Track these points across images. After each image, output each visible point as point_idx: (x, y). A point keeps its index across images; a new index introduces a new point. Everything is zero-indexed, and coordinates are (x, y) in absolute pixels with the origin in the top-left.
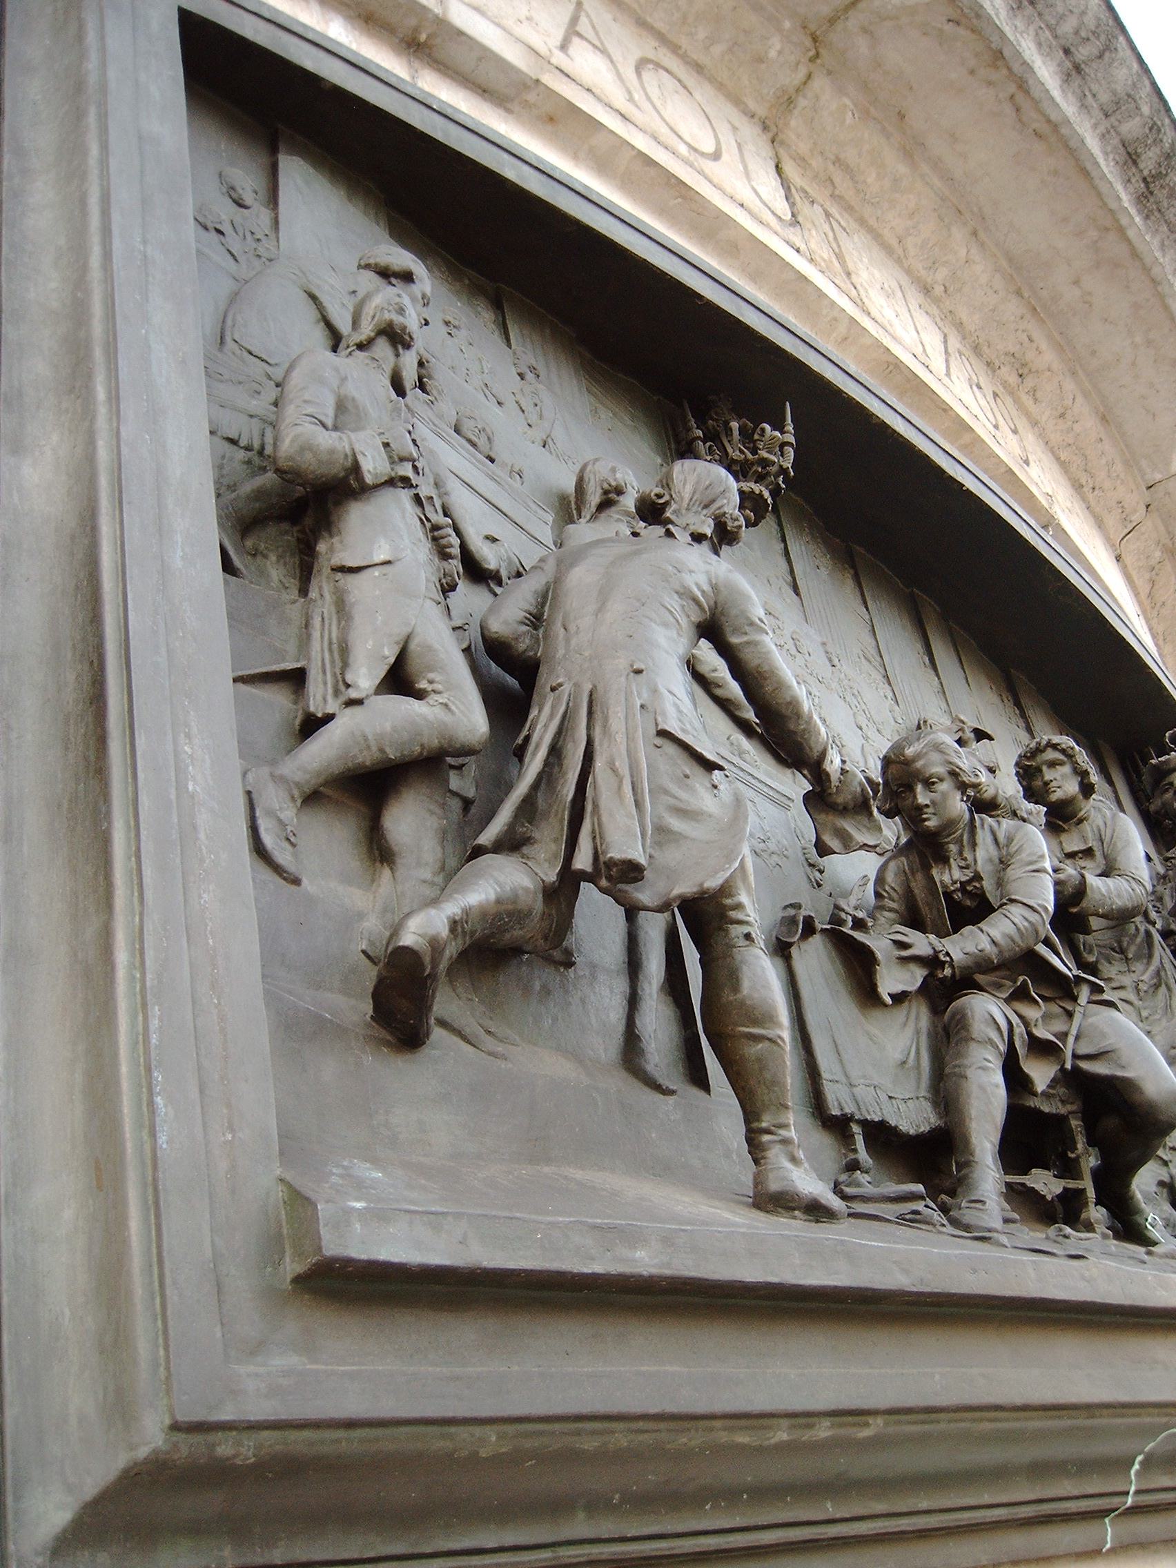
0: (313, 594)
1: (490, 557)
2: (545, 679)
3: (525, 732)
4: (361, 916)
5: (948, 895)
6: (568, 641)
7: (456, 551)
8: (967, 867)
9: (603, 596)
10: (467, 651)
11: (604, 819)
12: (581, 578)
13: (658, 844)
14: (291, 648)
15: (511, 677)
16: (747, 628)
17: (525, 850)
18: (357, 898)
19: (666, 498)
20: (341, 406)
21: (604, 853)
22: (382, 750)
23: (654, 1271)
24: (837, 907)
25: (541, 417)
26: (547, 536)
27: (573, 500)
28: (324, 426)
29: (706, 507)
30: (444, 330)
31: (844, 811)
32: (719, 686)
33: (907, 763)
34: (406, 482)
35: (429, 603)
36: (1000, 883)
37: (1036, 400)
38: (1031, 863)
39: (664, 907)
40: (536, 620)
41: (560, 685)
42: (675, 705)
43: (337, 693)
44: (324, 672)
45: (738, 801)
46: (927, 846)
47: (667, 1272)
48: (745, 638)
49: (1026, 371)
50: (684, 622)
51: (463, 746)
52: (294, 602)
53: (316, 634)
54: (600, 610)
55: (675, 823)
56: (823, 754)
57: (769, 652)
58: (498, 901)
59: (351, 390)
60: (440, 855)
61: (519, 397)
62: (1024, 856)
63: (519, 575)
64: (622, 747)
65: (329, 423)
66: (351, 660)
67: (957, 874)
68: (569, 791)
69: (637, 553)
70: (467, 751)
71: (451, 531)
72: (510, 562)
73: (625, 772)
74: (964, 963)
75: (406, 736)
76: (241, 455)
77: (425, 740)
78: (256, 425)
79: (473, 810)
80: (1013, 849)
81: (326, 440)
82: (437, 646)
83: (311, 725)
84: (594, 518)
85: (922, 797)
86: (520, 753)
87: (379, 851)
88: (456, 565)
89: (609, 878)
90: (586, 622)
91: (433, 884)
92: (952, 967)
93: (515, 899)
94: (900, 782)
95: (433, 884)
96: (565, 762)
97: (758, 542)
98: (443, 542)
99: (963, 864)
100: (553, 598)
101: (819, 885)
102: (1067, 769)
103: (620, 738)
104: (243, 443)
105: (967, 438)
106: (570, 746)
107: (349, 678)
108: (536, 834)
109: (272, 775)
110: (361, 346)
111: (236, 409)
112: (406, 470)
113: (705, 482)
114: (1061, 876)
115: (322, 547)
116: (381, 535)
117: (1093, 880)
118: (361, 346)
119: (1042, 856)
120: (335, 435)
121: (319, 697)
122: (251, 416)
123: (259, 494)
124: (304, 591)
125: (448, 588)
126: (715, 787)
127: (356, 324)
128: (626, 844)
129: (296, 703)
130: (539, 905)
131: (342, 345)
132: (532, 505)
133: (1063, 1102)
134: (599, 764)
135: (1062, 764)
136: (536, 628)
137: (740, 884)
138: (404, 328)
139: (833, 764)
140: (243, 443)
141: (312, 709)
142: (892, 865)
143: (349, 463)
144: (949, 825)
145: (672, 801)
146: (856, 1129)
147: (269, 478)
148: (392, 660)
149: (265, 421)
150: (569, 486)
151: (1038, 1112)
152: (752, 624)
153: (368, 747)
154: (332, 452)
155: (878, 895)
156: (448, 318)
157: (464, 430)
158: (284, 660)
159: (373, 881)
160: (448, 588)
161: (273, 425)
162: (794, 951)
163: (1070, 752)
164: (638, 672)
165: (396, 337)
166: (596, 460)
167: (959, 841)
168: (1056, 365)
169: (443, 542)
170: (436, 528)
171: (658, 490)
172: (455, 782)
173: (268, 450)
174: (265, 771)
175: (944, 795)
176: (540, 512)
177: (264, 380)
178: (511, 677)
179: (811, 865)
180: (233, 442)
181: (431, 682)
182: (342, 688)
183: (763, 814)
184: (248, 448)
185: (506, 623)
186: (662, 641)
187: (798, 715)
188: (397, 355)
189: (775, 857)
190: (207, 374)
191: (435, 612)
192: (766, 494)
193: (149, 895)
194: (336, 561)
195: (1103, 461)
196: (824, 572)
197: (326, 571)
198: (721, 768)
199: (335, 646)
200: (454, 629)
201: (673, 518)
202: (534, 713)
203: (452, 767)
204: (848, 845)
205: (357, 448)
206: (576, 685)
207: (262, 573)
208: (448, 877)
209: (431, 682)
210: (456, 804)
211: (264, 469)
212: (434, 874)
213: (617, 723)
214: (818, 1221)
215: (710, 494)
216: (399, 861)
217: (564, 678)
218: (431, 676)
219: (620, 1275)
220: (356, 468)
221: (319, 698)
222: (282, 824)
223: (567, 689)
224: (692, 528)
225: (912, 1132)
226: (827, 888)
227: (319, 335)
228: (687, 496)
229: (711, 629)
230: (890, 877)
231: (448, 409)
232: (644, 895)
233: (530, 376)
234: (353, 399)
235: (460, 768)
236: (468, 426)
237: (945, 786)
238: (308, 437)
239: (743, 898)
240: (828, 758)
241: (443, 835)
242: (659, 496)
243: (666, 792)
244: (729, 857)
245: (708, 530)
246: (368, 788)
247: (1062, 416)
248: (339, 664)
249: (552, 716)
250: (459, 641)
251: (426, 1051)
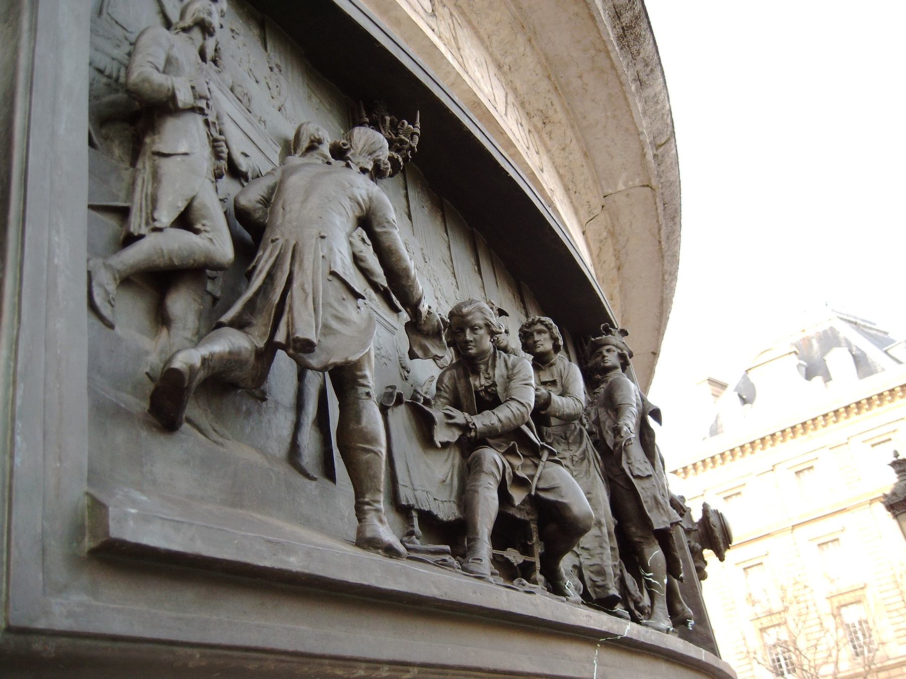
0: (139, 165)
1: (244, 165)
2: (268, 235)
3: (254, 264)
4: (147, 353)
5: (477, 392)
6: (284, 216)
7: (225, 156)
8: (489, 378)
9: (308, 193)
10: (225, 213)
11: (296, 315)
12: (295, 182)
13: (324, 335)
14: (123, 195)
15: (250, 229)
16: (386, 224)
17: (247, 329)
18: (146, 342)
19: (348, 146)
20: (169, 61)
21: (293, 334)
22: (171, 259)
23: (299, 570)
24: (416, 391)
25: (279, 94)
26: (276, 160)
27: (292, 143)
28: (158, 69)
29: (370, 154)
30: (230, 34)
31: (427, 335)
32: (362, 261)
33: (464, 316)
34: (201, 111)
35: (207, 181)
36: (506, 389)
37: (551, 138)
38: (524, 380)
39: (323, 370)
40: (267, 202)
41: (277, 239)
42: (341, 259)
43: (147, 224)
44: (141, 211)
45: (370, 318)
46: (468, 363)
47: (306, 571)
48: (384, 230)
49: (547, 121)
50: (351, 214)
51: (218, 263)
52: (126, 169)
53: (138, 189)
54: (305, 200)
55: (334, 324)
56: (420, 300)
57: (395, 239)
58: (230, 353)
59: (175, 52)
60: (197, 325)
61: (268, 80)
62: (521, 375)
63: (258, 177)
64: (309, 277)
65: (161, 68)
66: (158, 206)
67: (483, 382)
68: (276, 298)
69: (328, 173)
70: (219, 267)
71: (223, 144)
72: (254, 170)
73: (310, 291)
75: (186, 253)
76: (104, 80)
77: (197, 258)
78: (115, 65)
79: (218, 304)
80: (515, 371)
81: (158, 78)
82: (210, 205)
83: (130, 239)
84: (303, 155)
85: (469, 336)
86: (249, 276)
87: (161, 318)
88: (224, 164)
89: (295, 349)
90: (296, 206)
91: (191, 341)
92: (476, 431)
93: (239, 353)
94: (458, 326)
95: (191, 341)
96: (276, 282)
97: (393, 184)
98: (219, 149)
99: (487, 376)
100: (279, 191)
101: (406, 379)
102: (547, 336)
103: (309, 272)
104: (107, 73)
105: (512, 151)
106: (279, 273)
107: (156, 216)
108: (254, 322)
109: (104, 264)
110: (185, 30)
111: (104, 53)
112: (202, 104)
113: (371, 141)
114: (538, 393)
115: (148, 140)
116: (183, 138)
117: (555, 397)
118: (185, 30)
119: (531, 377)
120: (164, 76)
121: (137, 224)
122: (113, 59)
123: (112, 104)
124: (133, 164)
125: (218, 176)
126: (359, 308)
127: (182, 16)
128: (306, 330)
129: (122, 226)
130: (252, 359)
131: (172, 28)
132: (271, 142)
133: (528, 513)
134: (295, 285)
135: (545, 332)
136: (266, 207)
137: (366, 365)
138: (210, 24)
139: (424, 308)
140: (107, 73)
141: (132, 230)
142: (448, 373)
143: (170, 94)
144: (482, 353)
145: (334, 312)
146: (414, 514)
147: (121, 96)
148: (182, 209)
149: (121, 63)
150: (291, 136)
152: (388, 222)
153: (163, 256)
154: (161, 85)
155: (438, 389)
156: (234, 28)
157: (236, 91)
158: (117, 200)
159: (156, 335)
160: (218, 176)
161: (127, 67)
162: (390, 412)
164: (323, 237)
165: (205, 28)
166: (309, 123)
167: (486, 364)
168: (564, 121)
169: (219, 149)
170: (215, 140)
171: (344, 141)
172: (210, 287)
173: (122, 80)
174: (100, 261)
175: (481, 337)
176: (274, 146)
177: (123, 39)
178: (250, 229)
179: (403, 368)
180: (101, 71)
181: (204, 225)
182: (151, 221)
183: (380, 334)
184: (109, 77)
185: (249, 201)
186: (338, 222)
187: (408, 276)
188: (205, 39)
189: (384, 360)
190: (91, 31)
191: (209, 187)
192: (400, 160)
193: (24, 318)
194: (156, 148)
195: (583, 178)
196: (426, 210)
197: (148, 153)
198: (363, 298)
199: (149, 198)
200: (221, 200)
201: (351, 157)
202: (260, 253)
203: (210, 278)
204: (427, 354)
205: (176, 86)
206: (287, 241)
207: (110, 152)
208: (200, 338)
209: (204, 225)
210: (209, 299)
211: (117, 91)
212: (193, 335)
213: (308, 263)
214: (391, 557)
215: (374, 148)
216: (173, 325)
217: (283, 232)
218: (204, 222)
219: (280, 570)
220: (173, 98)
221: (136, 224)
222: (107, 293)
223: (281, 242)
224: (361, 165)
226: (410, 381)
227: (158, 19)
228: (360, 147)
229: (367, 221)
230: (446, 380)
231: (228, 78)
232: (314, 361)
233: (276, 70)
234: (177, 59)
235: (213, 279)
236: (238, 90)
237: (482, 332)
238: (147, 72)
239: (367, 373)
240: (422, 303)
241: (200, 315)
242: (344, 145)
243: (332, 306)
244: (364, 345)
245: (370, 167)
246: (157, 282)
247: (563, 149)
248: (150, 207)
249: (270, 256)
250: (223, 207)
251: (178, 435)
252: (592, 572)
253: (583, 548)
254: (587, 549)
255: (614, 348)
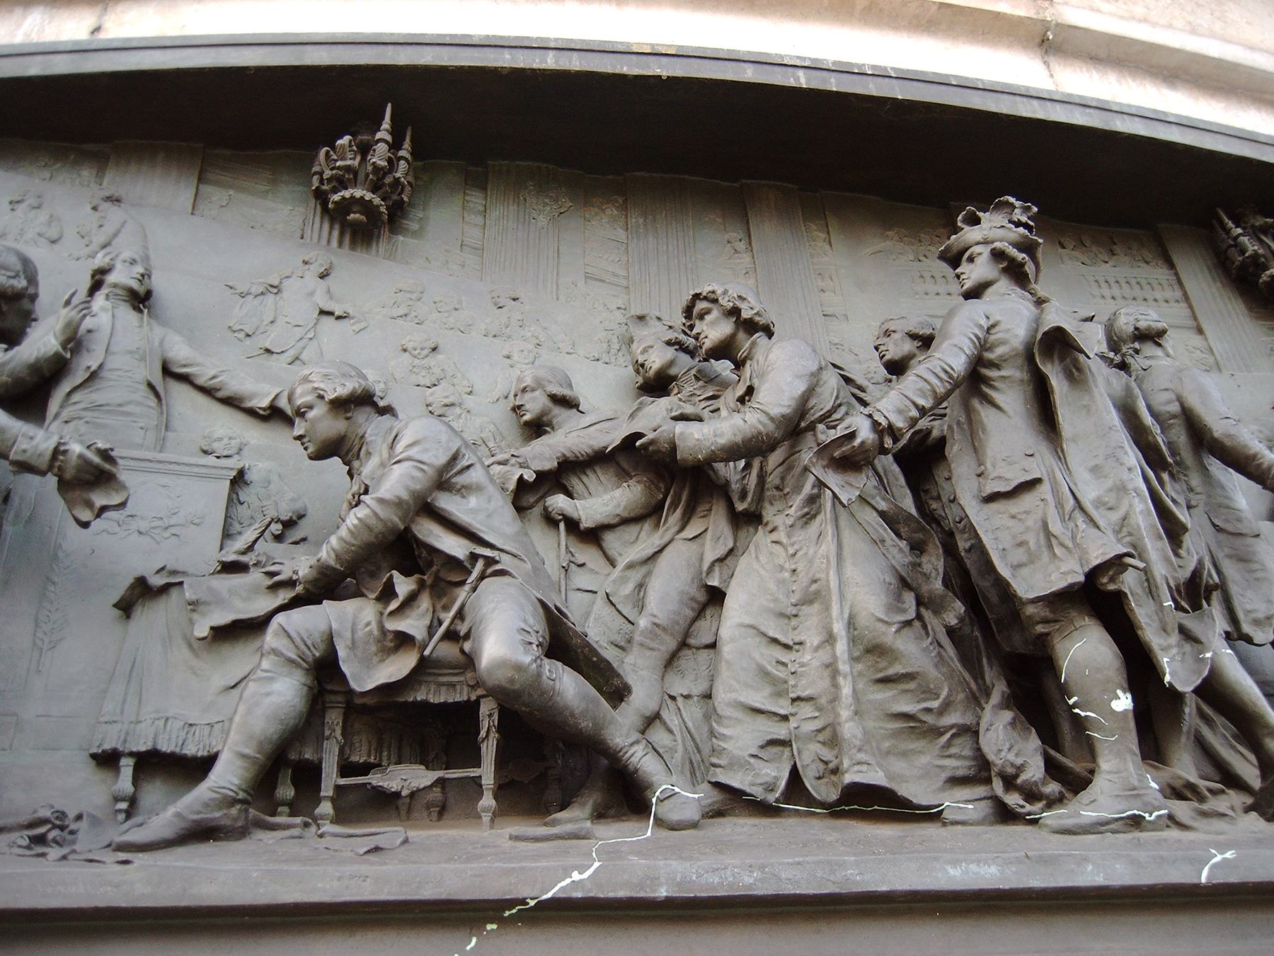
74: (310, 577)
135: (708, 312)
151: (425, 704)
163: (713, 296)
196: (542, 220)
225: (200, 754)
252: (824, 743)
253: (798, 699)
254: (809, 699)
255: (977, 249)
